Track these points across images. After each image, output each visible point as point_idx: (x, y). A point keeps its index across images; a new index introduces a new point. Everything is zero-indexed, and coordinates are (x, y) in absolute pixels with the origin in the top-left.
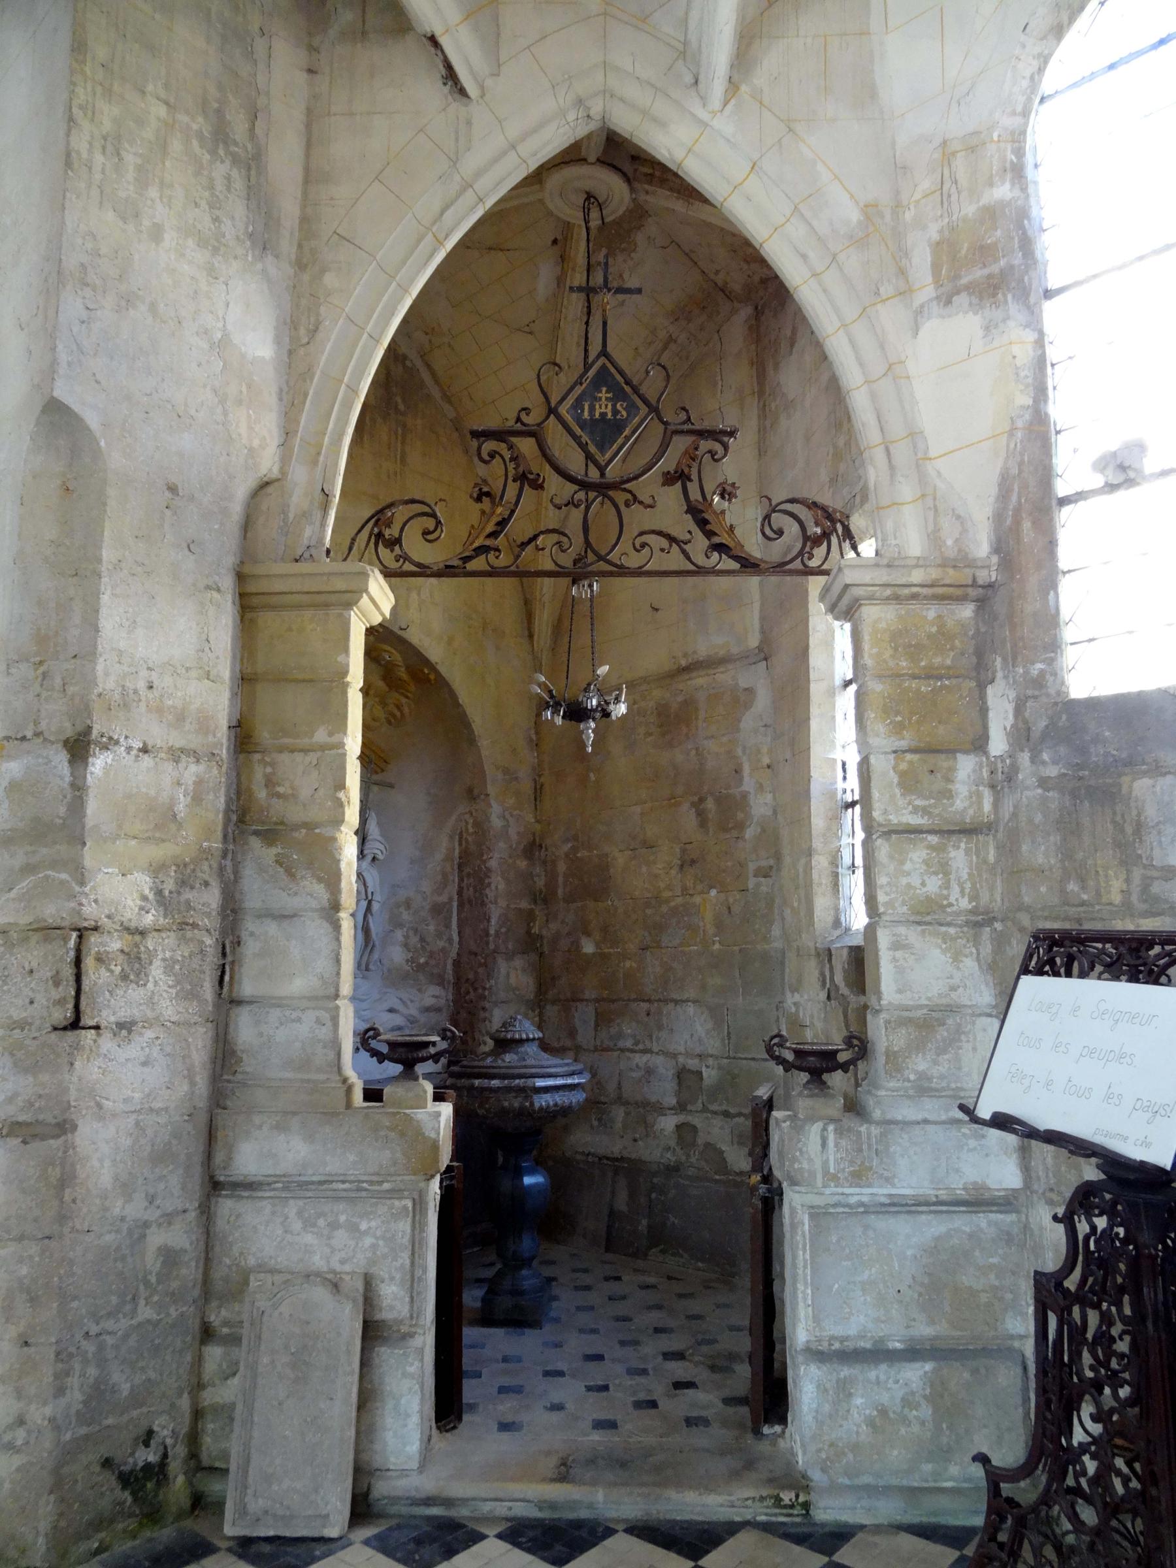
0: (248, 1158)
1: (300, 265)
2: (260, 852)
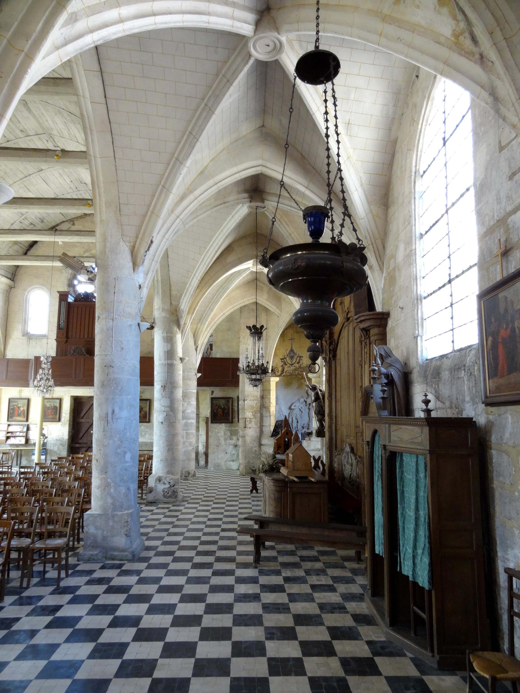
2: (264, 410)
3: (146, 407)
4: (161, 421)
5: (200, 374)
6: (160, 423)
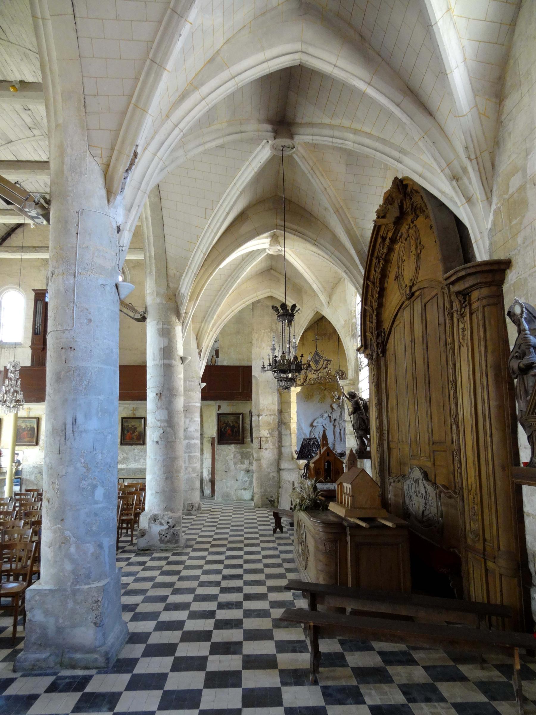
0: (284, 465)
2: (283, 426)
3: (140, 426)
4: (155, 440)
5: (204, 385)
6: (155, 443)
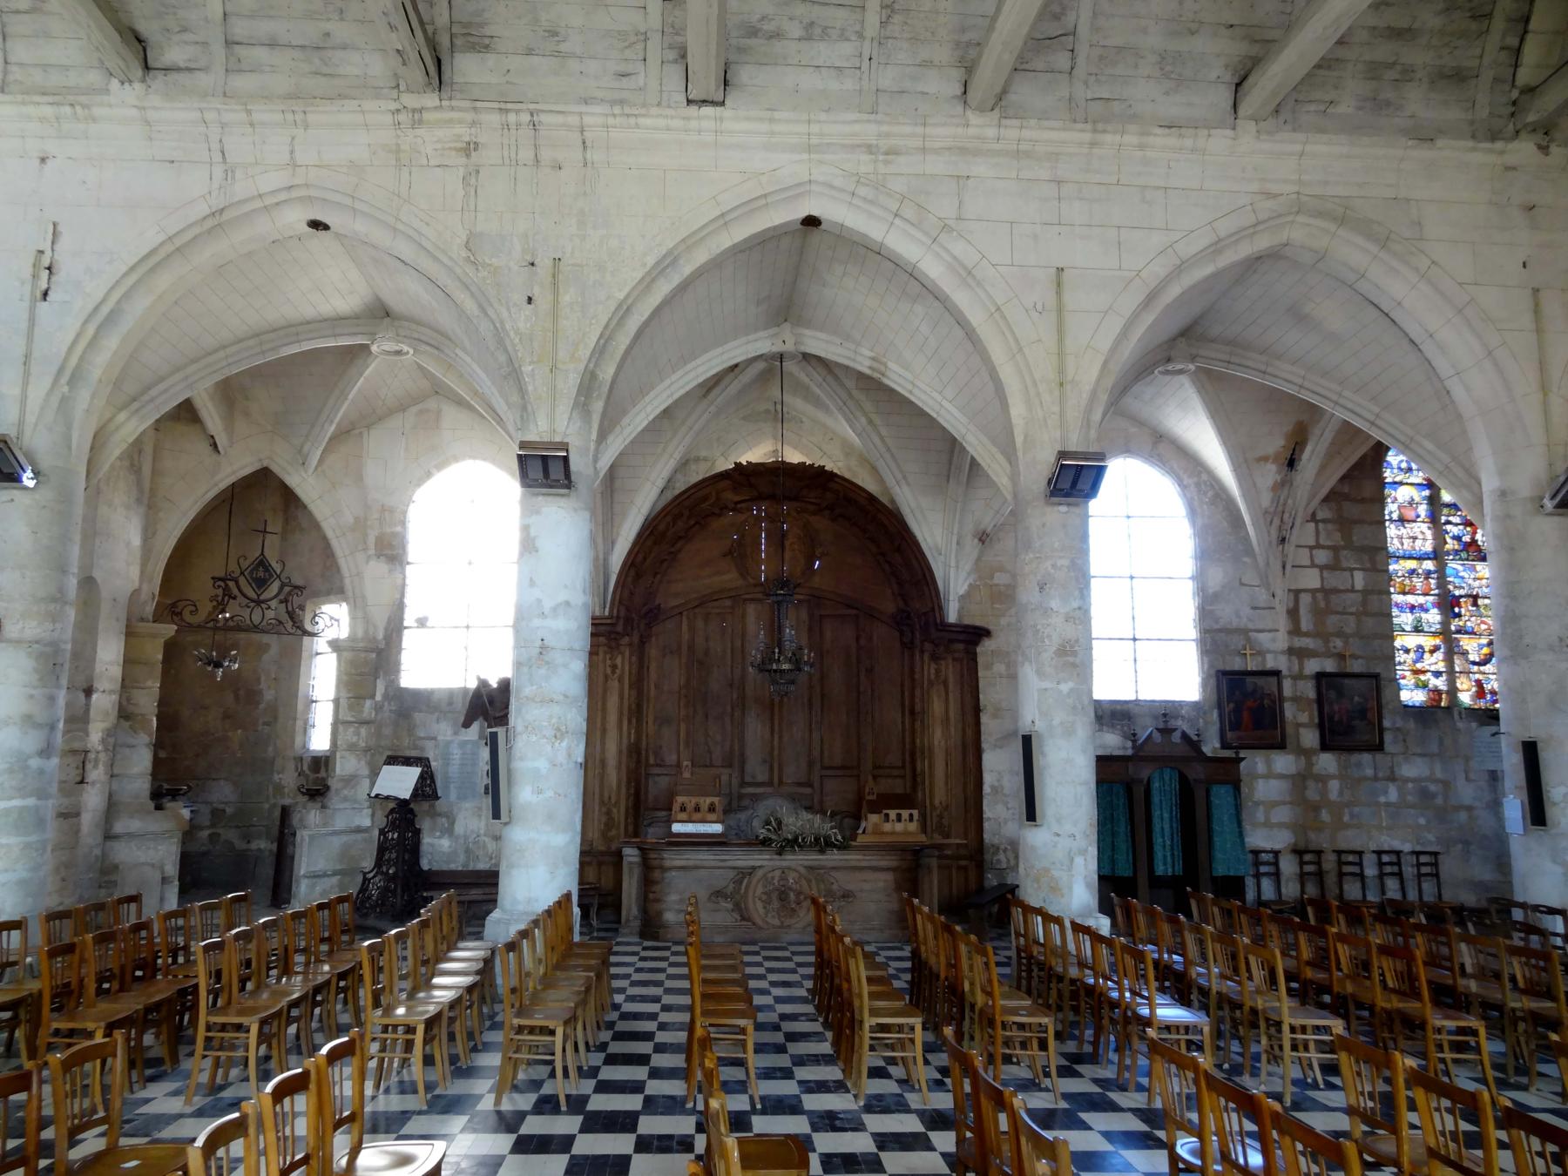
1: (150, 507)
